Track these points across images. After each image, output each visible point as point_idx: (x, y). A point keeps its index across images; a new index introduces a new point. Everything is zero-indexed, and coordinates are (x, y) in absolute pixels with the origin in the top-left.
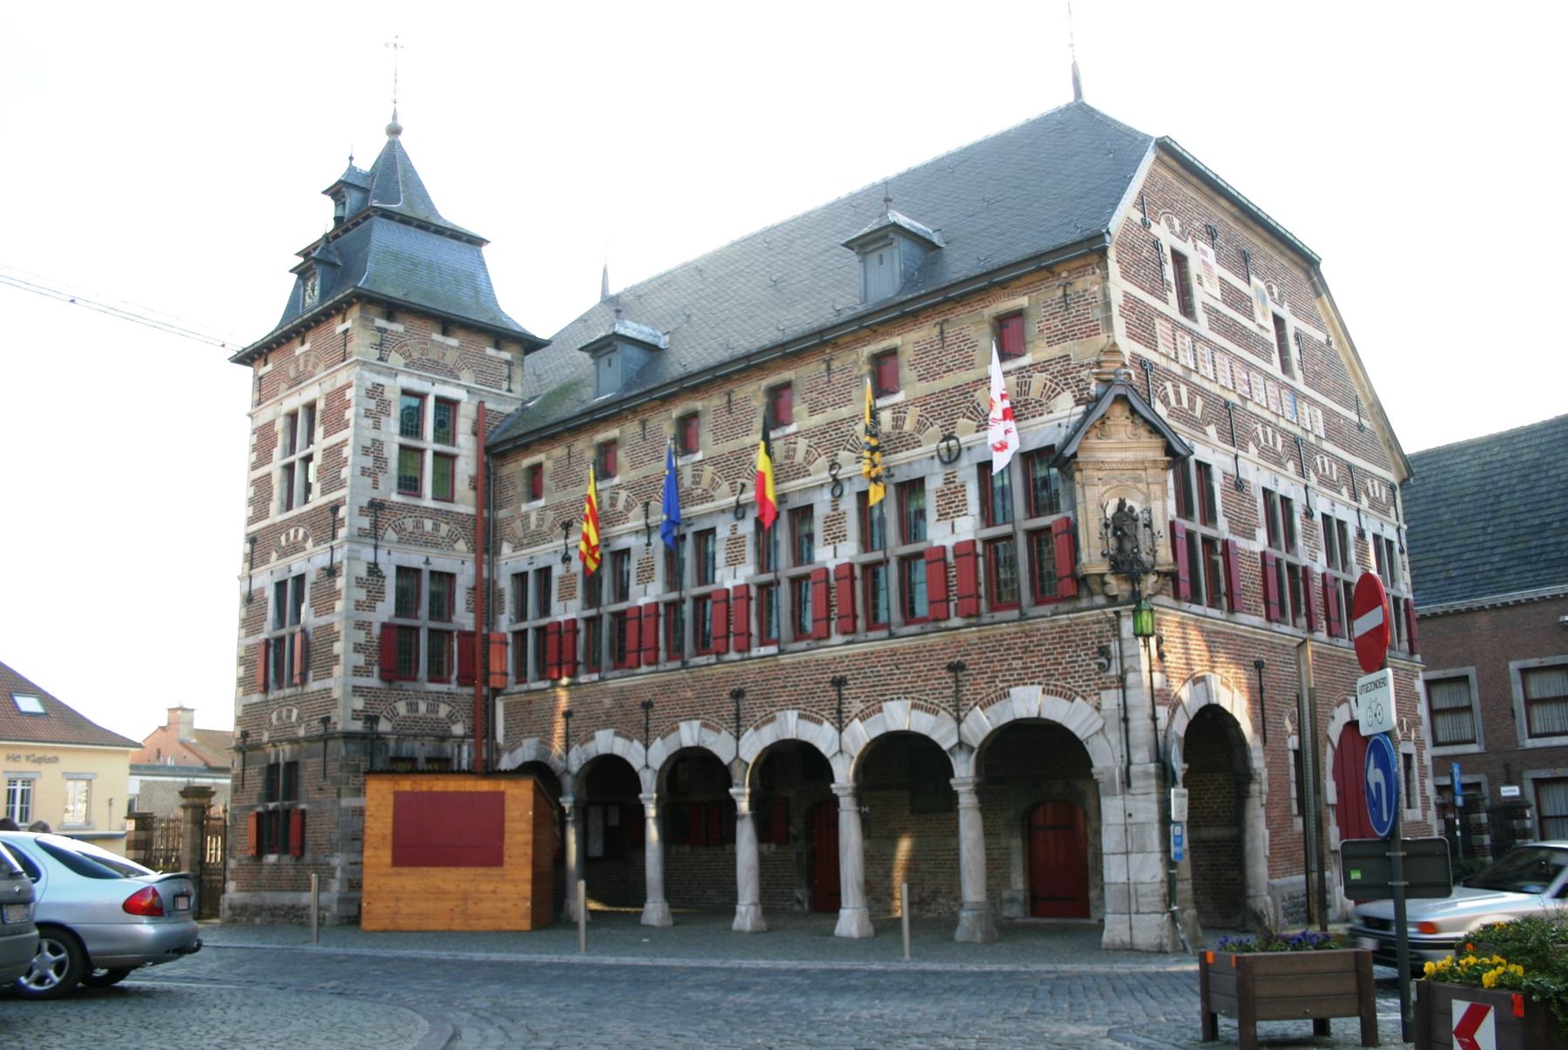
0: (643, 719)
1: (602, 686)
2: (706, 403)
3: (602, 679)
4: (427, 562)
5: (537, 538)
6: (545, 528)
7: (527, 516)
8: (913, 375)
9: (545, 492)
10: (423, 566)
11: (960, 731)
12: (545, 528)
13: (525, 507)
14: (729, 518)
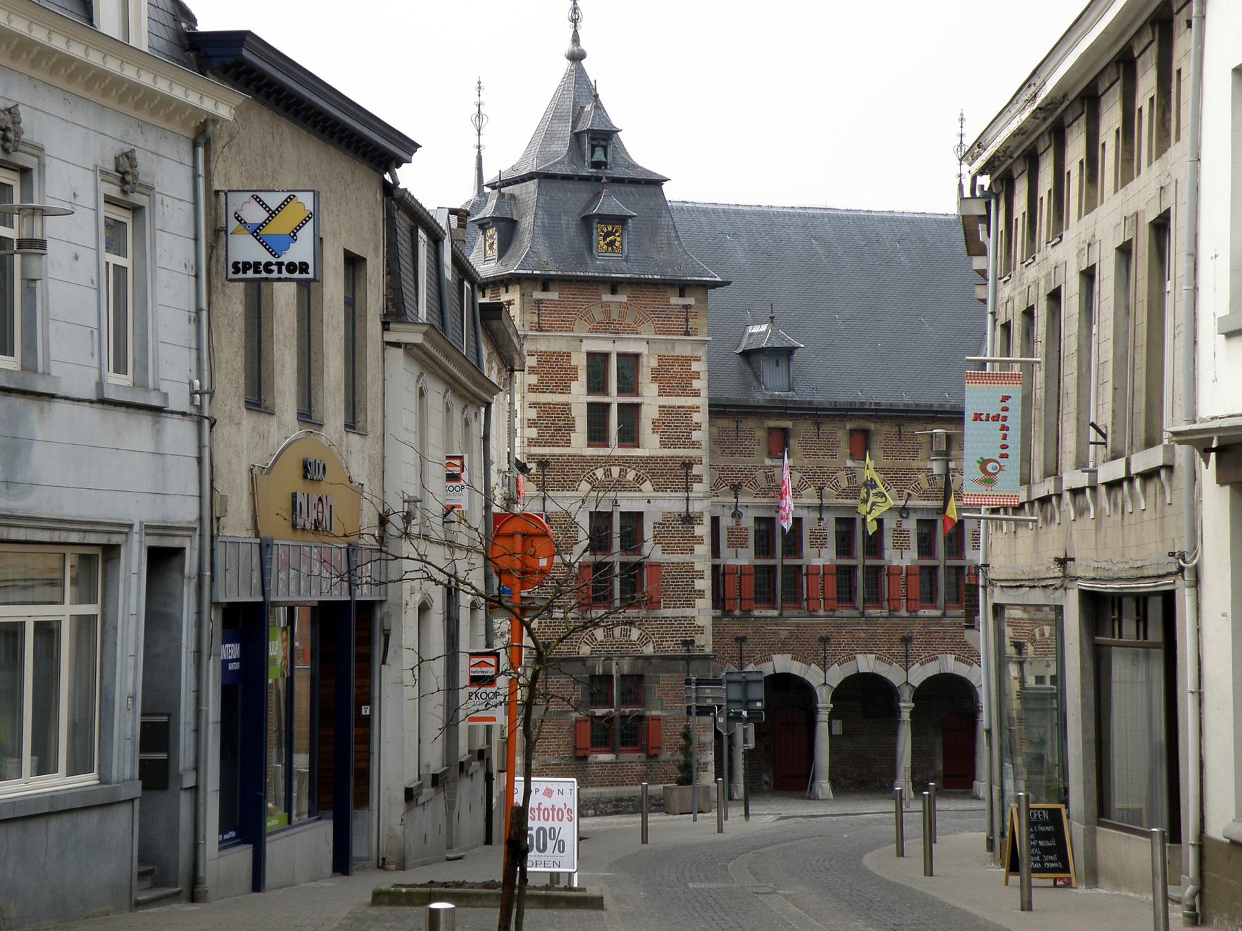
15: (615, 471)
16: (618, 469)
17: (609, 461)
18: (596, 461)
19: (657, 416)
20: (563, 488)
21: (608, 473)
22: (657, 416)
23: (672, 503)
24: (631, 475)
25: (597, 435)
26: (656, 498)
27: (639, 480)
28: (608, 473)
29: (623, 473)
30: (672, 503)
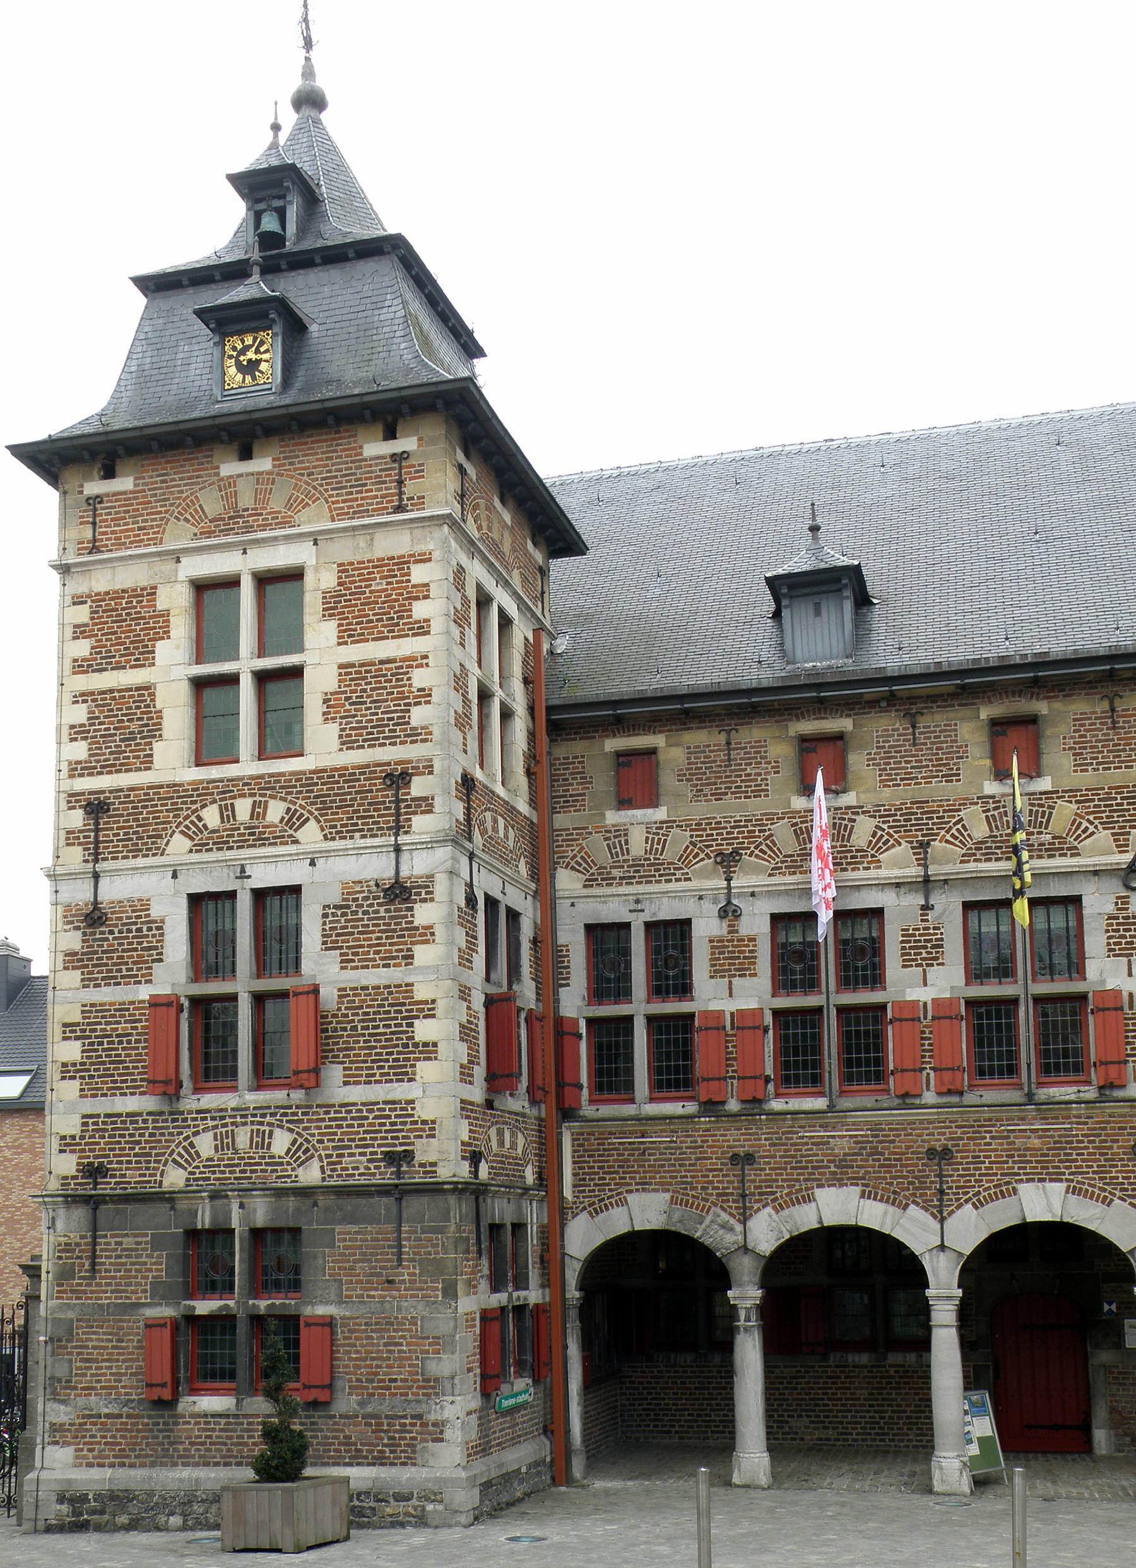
5: (650, 868)
6: (667, 856)
7: (621, 833)
9: (663, 799)
10: (496, 893)
12: (667, 856)
13: (612, 817)
15: (243, 808)
16: (248, 802)
17: (227, 791)
18: (202, 793)
20: (136, 852)
21: (227, 813)
23: (366, 862)
25: (212, 743)
26: (327, 854)
27: (294, 820)
28: (227, 813)
29: (259, 811)
30: (366, 862)
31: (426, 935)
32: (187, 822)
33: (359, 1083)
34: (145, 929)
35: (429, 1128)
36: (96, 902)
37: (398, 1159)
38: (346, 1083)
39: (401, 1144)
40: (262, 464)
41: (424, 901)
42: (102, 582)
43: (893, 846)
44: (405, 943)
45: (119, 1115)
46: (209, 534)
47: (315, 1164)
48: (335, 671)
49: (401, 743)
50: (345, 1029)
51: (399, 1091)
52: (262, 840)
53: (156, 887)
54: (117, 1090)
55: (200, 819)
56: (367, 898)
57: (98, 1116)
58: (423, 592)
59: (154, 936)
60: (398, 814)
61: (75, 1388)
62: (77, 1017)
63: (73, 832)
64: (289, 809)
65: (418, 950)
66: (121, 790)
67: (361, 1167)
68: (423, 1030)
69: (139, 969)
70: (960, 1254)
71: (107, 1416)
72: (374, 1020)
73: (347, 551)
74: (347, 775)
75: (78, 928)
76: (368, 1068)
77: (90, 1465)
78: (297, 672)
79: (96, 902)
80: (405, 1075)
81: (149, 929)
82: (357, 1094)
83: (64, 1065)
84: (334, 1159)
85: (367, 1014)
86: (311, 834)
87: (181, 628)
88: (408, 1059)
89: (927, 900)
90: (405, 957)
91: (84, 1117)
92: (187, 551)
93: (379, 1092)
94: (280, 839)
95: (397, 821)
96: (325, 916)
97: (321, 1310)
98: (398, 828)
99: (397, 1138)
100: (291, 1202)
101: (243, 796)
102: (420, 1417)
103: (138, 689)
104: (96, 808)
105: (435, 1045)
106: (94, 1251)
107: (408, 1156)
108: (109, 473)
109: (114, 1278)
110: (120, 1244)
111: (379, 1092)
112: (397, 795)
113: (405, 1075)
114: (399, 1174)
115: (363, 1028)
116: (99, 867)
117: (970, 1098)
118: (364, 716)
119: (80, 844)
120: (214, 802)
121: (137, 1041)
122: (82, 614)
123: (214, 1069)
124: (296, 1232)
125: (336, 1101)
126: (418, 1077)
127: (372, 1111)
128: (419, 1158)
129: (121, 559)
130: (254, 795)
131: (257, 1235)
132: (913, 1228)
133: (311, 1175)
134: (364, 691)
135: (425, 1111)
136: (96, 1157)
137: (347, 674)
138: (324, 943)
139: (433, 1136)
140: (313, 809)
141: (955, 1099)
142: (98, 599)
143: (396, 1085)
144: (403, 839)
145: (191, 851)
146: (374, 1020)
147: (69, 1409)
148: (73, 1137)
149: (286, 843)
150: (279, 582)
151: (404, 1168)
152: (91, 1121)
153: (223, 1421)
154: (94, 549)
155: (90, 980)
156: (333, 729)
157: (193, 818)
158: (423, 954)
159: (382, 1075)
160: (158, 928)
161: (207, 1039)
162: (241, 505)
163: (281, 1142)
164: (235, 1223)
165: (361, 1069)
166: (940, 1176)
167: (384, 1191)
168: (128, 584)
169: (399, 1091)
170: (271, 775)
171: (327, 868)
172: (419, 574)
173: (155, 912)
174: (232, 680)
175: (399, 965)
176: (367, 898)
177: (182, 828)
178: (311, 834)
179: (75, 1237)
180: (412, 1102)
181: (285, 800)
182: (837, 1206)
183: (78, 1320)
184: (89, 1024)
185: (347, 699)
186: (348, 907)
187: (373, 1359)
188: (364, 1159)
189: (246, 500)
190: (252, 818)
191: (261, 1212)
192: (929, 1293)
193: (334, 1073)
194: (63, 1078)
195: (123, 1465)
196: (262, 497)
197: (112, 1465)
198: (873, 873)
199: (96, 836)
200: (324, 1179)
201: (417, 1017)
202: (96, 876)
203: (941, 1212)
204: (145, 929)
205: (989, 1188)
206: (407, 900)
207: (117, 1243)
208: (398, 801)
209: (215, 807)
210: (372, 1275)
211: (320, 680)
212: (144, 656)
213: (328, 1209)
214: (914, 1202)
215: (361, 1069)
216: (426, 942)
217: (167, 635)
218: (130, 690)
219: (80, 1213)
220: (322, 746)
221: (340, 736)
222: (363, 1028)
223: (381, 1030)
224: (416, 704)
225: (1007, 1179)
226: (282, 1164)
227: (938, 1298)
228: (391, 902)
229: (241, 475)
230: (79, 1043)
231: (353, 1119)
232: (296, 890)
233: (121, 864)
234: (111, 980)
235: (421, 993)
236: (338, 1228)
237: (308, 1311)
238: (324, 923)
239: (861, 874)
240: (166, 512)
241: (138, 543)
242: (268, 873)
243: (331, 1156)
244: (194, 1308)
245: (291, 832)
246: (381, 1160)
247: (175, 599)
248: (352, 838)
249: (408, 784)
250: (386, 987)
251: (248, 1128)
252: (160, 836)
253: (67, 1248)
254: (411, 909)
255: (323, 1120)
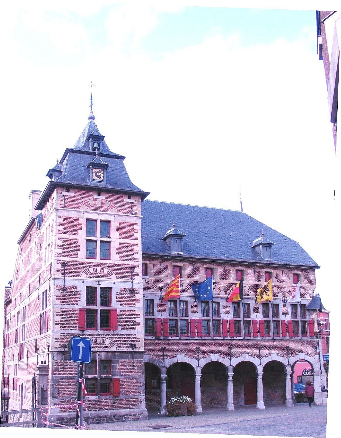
0: (197, 353)
1: (180, 341)
2: (216, 267)
3: (180, 339)
4: (99, 284)
8: (276, 280)
11: (231, 362)
14: (224, 300)
15: (99, 269)
16: (100, 268)
17: (95, 265)
18: (90, 264)
19: (118, 247)
20: (74, 275)
21: (95, 270)
22: (118, 247)
23: (124, 284)
24: (106, 271)
25: (91, 254)
27: (110, 273)
28: (95, 270)
29: (102, 270)
30: (124, 284)
31: (138, 301)
32: (86, 271)
33: (124, 330)
34: (76, 293)
35: (138, 340)
36: (64, 285)
37: (133, 346)
38: (121, 330)
39: (133, 343)
40: (103, 197)
41: (137, 294)
42: (66, 214)
43: (190, 289)
44: (134, 302)
45: (70, 334)
46: (91, 209)
47: (115, 347)
48: (119, 244)
49: (132, 261)
50: (121, 319)
51: (133, 332)
52: (103, 277)
53: (80, 283)
54: (69, 328)
55: (89, 270)
56: (126, 292)
57: (65, 334)
58: (136, 231)
59: (78, 295)
60: (132, 276)
61: (59, 395)
62: (60, 311)
63: (58, 269)
64: (109, 271)
65: (136, 303)
66: (70, 261)
67: (124, 348)
68: (137, 320)
69: (75, 302)
70: (201, 367)
71: (67, 401)
72: (127, 317)
73: (121, 219)
74: (122, 266)
75: (60, 291)
76: (126, 327)
77: (64, 412)
78: (109, 242)
79: (64, 285)
80: (133, 329)
81: (77, 293)
82: (124, 332)
83: (56, 322)
84: (119, 346)
85: (126, 316)
86: (114, 277)
87: (84, 228)
88: (134, 326)
89: (195, 300)
90: (134, 305)
91: (61, 334)
92: (86, 212)
93: (128, 332)
94: (107, 277)
95: (132, 277)
96: (117, 294)
97: (116, 377)
98: (132, 278)
99: (132, 342)
100: (110, 354)
101: (99, 267)
102: (137, 399)
103: (74, 240)
104: (64, 264)
105: (140, 323)
106: (64, 364)
107: (135, 345)
108: (68, 191)
109: (69, 370)
110: (70, 363)
111: (128, 332)
112: (132, 271)
113: (133, 329)
114: (133, 349)
115: (125, 319)
116: (66, 277)
117: (203, 338)
118: (124, 254)
119: (60, 272)
120: (92, 267)
121: (74, 318)
122: (61, 221)
123: (92, 325)
124: (111, 361)
125: (119, 333)
126: (136, 330)
127: (127, 336)
128: (137, 346)
129: (71, 210)
130: (101, 267)
131: (102, 361)
132: (193, 362)
133: (114, 349)
134: (125, 249)
135: (138, 336)
136: (64, 343)
137: (121, 245)
138: (117, 300)
139: (140, 342)
140: (114, 272)
141: (200, 338)
142: (65, 218)
143: (132, 331)
144: (133, 281)
145: (87, 277)
146: (127, 317)
147: (58, 400)
148: (58, 338)
149: (108, 278)
150: (106, 223)
151: (134, 348)
152: (63, 335)
153: (95, 401)
154: (65, 207)
155: (63, 303)
156: (118, 256)
157: (87, 270)
158: (137, 304)
159: (129, 329)
160: (79, 293)
161: (88, 319)
162: (98, 205)
163: (107, 342)
164: (97, 359)
165: (125, 327)
166: (198, 353)
167: (130, 352)
168: (72, 216)
169: (133, 332)
170: (105, 263)
171: (118, 285)
172: (135, 227)
173: (79, 289)
174: (96, 241)
175: (132, 306)
176: (126, 292)
177: (85, 272)
178: (114, 277)
179: (59, 361)
180: (135, 334)
181: (108, 269)
182: (181, 358)
183: (60, 380)
184: (62, 313)
185: (121, 250)
186: (122, 293)
187: (127, 387)
188: (125, 346)
189: (99, 204)
190: (101, 272)
191: (103, 356)
192: (196, 375)
193: (119, 328)
194: (56, 325)
195: (71, 412)
196: (103, 204)
197: (69, 412)
198: (186, 294)
199: (64, 271)
200: (117, 350)
201: (136, 317)
202: (64, 280)
203: (198, 360)
204: (76, 293)
205: (206, 355)
206: (134, 293)
207: (69, 363)
208: (132, 273)
209: (92, 268)
210: (127, 370)
211: (115, 245)
212: (75, 233)
213: (118, 356)
214: (194, 358)
215: (125, 327)
216: (138, 302)
217: (81, 229)
218: (72, 239)
219: (60, 355)
220: (115, 259)
221: (120, 258)
222: (125, 319)
223: (129, 319)
224: (135, 254)
225: (209, 353)
226: (108, 346)
227: (197, 376)
228: (131, 293)
229: (98, 199)
230: (60, 317)
231: (123, 337)
232: (110, 289)
233: (70, 278)
234: (67, 303)
235: (137, 312)
236: (120, 360)
237: (114, 377)
238: (117, 296)
239: (184, 294)
240: (81, 202)
241: (74, 208)
242: (105, 283)
243: (118, 345)
244: (88, 377)
245: (109, 276)
246: (129, 346)
247: (83, 222)
248: (122, 279)
249: (134, 270)
250: (130, 311)
251: (100, 338)
252: (80, 273)
253: (57, 363)
254: (135, 295)
255: (117, 337)
